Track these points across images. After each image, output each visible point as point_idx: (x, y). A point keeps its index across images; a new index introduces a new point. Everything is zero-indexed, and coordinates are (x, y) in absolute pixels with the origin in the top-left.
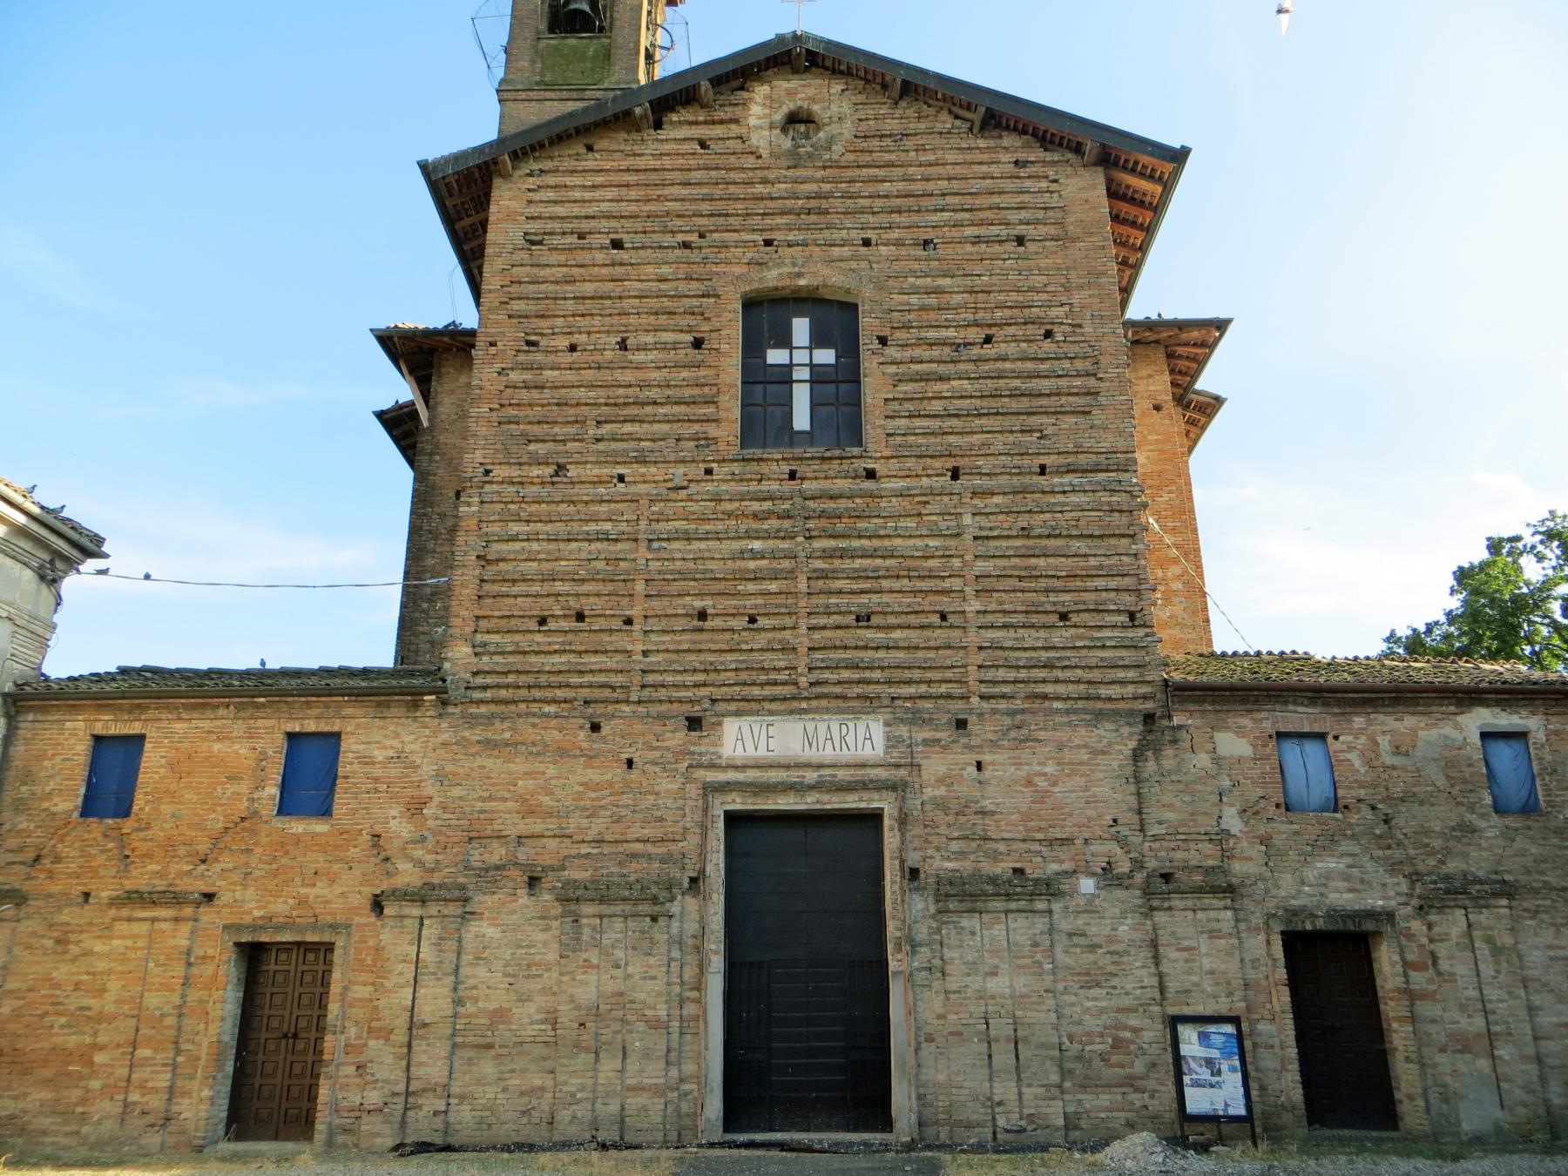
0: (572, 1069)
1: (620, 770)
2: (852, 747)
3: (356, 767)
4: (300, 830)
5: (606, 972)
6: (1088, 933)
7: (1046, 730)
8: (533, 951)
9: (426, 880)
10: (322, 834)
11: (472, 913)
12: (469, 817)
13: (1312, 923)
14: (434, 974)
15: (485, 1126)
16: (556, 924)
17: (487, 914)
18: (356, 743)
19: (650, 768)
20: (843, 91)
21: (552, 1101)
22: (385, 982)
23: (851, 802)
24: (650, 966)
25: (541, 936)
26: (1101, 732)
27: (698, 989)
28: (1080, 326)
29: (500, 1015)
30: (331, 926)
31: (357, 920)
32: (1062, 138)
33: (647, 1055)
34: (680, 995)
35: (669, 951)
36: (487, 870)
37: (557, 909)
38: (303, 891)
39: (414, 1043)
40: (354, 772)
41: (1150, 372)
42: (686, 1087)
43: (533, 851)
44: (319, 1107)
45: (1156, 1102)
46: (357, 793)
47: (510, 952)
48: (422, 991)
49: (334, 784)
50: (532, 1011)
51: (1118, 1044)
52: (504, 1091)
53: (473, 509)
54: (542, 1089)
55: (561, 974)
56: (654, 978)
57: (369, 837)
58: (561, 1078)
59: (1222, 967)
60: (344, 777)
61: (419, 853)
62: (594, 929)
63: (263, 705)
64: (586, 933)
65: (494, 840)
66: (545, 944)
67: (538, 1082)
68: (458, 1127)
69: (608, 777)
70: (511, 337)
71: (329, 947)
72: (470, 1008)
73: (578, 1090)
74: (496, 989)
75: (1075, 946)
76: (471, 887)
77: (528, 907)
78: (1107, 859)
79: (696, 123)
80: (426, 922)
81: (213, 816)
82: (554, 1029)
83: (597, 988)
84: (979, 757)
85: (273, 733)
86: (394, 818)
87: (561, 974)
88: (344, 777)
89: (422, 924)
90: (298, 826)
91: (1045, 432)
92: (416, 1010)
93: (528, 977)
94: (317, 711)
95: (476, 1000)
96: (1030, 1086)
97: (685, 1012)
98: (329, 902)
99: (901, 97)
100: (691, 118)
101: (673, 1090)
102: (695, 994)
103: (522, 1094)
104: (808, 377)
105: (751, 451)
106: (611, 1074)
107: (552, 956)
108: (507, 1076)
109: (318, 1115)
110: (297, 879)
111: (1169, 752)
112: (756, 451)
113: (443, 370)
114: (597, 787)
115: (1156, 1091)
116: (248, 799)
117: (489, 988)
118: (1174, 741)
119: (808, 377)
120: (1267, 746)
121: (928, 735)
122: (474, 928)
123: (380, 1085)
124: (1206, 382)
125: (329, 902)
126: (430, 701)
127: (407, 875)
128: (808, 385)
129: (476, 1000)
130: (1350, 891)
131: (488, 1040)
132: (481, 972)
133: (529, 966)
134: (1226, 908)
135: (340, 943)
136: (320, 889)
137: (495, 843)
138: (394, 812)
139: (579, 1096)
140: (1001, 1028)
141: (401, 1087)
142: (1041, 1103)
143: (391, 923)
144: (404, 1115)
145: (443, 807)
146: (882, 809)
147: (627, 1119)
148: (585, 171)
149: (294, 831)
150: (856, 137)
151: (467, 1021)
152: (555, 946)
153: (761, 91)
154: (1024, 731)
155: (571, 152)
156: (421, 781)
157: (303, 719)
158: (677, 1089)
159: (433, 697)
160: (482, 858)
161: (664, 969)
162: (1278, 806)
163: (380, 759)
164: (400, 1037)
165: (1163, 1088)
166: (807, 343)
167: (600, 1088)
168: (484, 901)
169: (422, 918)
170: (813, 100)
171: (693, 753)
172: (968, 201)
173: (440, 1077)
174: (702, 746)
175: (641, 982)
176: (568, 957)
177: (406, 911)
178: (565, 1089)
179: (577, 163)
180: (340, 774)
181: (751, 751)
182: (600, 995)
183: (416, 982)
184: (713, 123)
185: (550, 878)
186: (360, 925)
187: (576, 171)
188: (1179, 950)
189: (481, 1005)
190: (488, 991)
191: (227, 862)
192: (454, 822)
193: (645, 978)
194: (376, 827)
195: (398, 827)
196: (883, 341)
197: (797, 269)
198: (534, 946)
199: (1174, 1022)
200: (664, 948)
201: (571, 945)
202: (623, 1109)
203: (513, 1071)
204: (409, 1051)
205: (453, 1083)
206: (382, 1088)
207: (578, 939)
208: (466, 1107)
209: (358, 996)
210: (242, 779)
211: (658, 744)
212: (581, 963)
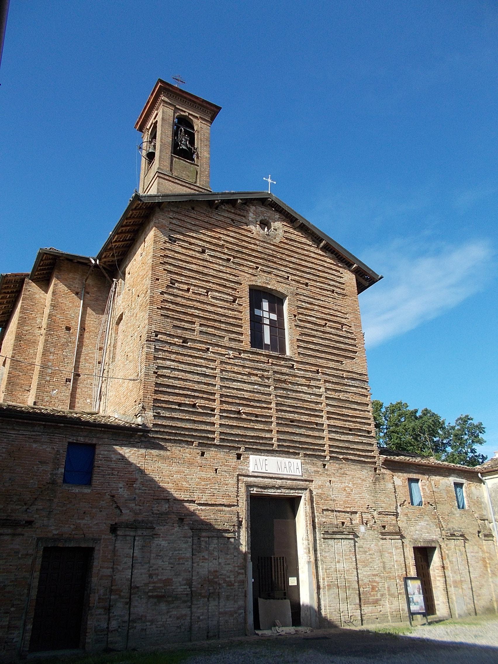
0: (198, 606)
1: (213, 474)
2: (293, 472)
3: (103, 462)
4: (77, 491)
5: (211, 562)
6: (364, 547)
7: (349, 471)
8: (181, 552)
13: (420, 544)
14: (140, 563)
15: (162, 635)
17: (162, 535)
18: (103, 450)
22: (118, 567)
24: (227, 559)
25: (184, 546)
26: (363, 473)
28: (351, 327)
29: (168, 582)
31: (103, 536)
37: (190, 533)
39: (132, 596)
40: (102, 464)
44: (88, 631)
45: (383, 609)
46: (104, 475)
47: (171, 553)
48: (135, 571)
50: (181, 580)
51: (373, 588)
52: (170, 617)
53: (152, 350)
54: (185, 615)
56: (229, 564)
57: (109, 497)
58: (194, 610)
59: (399, 559)
60: (98, 467)
62: (206, 542)
66: (186, 549)
67: (184, 612)
69: (209, 476)
72: (155, 579)
74: (166, 570)
76: (155, 522)
77: (178, 532)
78: (366, 520)
79: (230, 212)
80: (137, 538)
81: (31, 481)
83: (208, 569)
86: (121, 488)
88: (98, 467)
89: (134, 540)
90: (76, 490)
91: (343, 362)
92: (133, 580)
93: (179, 564)
94: (85, 434)
95: (157, 575)
96: (351, 605)
100: (229, 210)
101: (236, 613)
103: (178, 618)
106: (213, 607)
111: (382, 482)
112: (258, 350)
114: (204, 479)
115: (383, 605)
116: (51, 474)
117: (162, 569)
121: (316, 469)
122: (156, 541)
123: (116, 617)
125: (91, 527)
127: (127, 516)
129: (157, 575)
130: (428, 533)
131: (163, 594)
132: (160, 562)
135: (97, 548)
137: (163, 502)
138: (121, 485)
142: (354, 611)
144: (128, 631)
145: (142, 484)
149: (74, 491)
151: (154, 585)
154: (343, 470)
155: (186, 208)
157: (78, 436)
160: (158, 508)
163: (114, 459)
164: (125, 593)
168: (161, 529)
169: (135, 537)
170: (269, 217)
171: (239, 469)
173: (143, 612)
174: (242, 467)
175: (224, 566)
182: (209, 572)
184: (236, 214)
185: (187, 520)
188: (388, 553)
189: (159, 577)
190: (162, 571)
191: (39, 505)
192: (147, 491)
193: (226, 564)
194: (112, 492)
195: (123, 492)
197: (267, 281)
198: (181, 550)
203: (173, 608)
204: (130, 600)
206: (118, 619)
207: (200, 547)
208: (154, 626)
210: (48, 463)
211: (227, 463)
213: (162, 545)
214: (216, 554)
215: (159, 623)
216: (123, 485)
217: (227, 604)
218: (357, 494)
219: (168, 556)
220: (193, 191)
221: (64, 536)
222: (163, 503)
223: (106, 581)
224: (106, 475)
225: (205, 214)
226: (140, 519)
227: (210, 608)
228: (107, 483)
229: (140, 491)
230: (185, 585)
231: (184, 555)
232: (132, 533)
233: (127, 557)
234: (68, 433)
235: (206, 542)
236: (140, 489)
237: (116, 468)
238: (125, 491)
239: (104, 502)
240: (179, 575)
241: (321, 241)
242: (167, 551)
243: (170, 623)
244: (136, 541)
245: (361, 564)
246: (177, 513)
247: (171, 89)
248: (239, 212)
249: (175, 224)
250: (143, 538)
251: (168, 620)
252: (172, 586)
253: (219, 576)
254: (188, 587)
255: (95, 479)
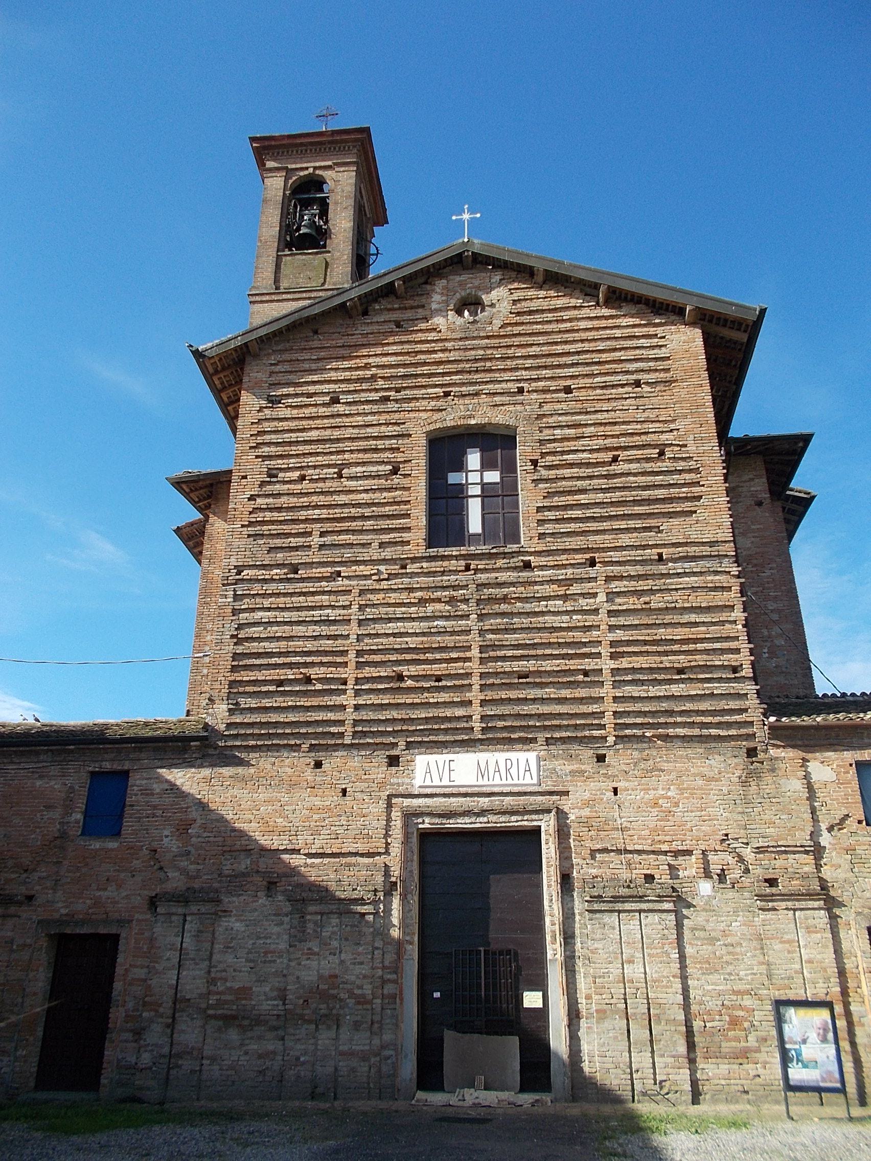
0: (297, 1037)
1: (337, 798)
2: (515, 777)
3: (140, 798)
5: (325, 958)
7: (668, 762)
8: (268, 941)
9: (188, 885)
10: (112, 850)
11: (225, 911)
12: (223, 835)
14: (193, 959)
16: (286, 919)
17: (235, 912)
19: (359, 796)
20: (501, 280)
21: (282, 1063)
22: (157, 965)
23: (515, 822)
25: (276, 929)
26: (712, 762)
27: (396, 973)
28: (686, 446)
29: (244, 993)
30: (118, 921)
31: (137, 916)
32: (668, 305)
33: (357, 1026)
34: (382, 977)
35: (373, 941)
36: (236, 876)
37: (287, 907)
38: (98, 894)
39: (177, 1015)
41: (751, 476)
42: (387, 1053)
43: (271, 861)
44: (105, 1065)
45: (768, 1071)
46: (140, 818)
47: (251, 942)
48: (184, 973)
49: (123, 811)
50: (267, 989)
51: (734, 1022)
52: (246, 1053)
53: (229, 600)
54: (274, 1053)
55: (290, 960)
56: (362, 963)
58: (289, 1044)
60: (131, 806)
61: (184, 864)
62: (315, 923)
63: (72, 751)
64: (310, 927)
65: (243, 853)
66: (279, 934)
68: (208, 1083)
69: (328, 803)
70: (256, 470)
71: (115, 938)
72: (220, 987)
73: (301, 1054)
74: (240, 971)
75: (697, 939)
77: (265, 906)
78: (721, 867)
80: (188, 918)
81: (33, 836)
82: (284, 1004)
83: (318, 971)
84: (615, 785)
85: (79, 772)
86: (167, 836)
87: (290, 960)
89: (185, 921)
90: (96, 845)
91: (661, 528)
92: (179, 988)
93: (265, 962)
95: (226, 980)
96: (662, 1056)
97: (386, 992)
98: (117, 903)
99: (544, 283)
100: (389, 306)
101: (376, 1055)
102: (394, 976)
104: (479, 493)
105: (435, 550)
106: (327, 1042)
107: (283, 946)
108: (247, 1042)
109: (103, 1072)
110: (93, 885)
111: (768, 778)
112: (441, 550)
113: (219, 496)
115: (766, 1063)
116: (60, 823)
117: (235, 970)
118: (773, 770)
119: (479, 493)
120: (848, 772)
121: (575, 767)
122: (224, 923)
124: (800, 483)
125: (117, 903)
126: (195, 746)
127: (175, 881)
128: (480, 499)
131: (233, 1013)
132: (230, 958)
133: (266, 953)
134: (820, 909)
135: (123, 935)
136: (110, 892)
138: (166, 833)
139: (302, 1059)
140: (638, 1007)
141: (166, 1050)
142: (671, 1071)
143: (162, 918)
144: (168, 1072)
145: (204, 827)
146: (540, 827)
147: (340, 1079)
148: (312, 349)
149: (92, 847)
150: (511, 313)
151: (218, 997)
152: (286, 937)
153: (441, 284)
154: (651, 762)
155: (301, 336)
156: (187, 808)
157: (102, 761)
158: (379, 1054)
159: (197, 743)
161: (370, 957)
162: (860, 822)
163: (158, 791)
164: (166, 1008)
165: (773, 1060)
166: (479, 468)
167: (319, 1053)
168: (232, 902)
169: (185, 915)
171: (392, 784)
172: (596, 357)
173: (196, 1042)
174: (397, 780)
175: (352, 967)
176: (295, 946)
177: (174, 910)
178: (292, 1053)
179: (306, 344)
180: (127, 803)
181: (436, 782)
182: (321, 977)
183: (179, 966)
184: (406, 309)
185: (283, 883)
186: (138, 920)
187: (305, 349)
188: (781, 942)
189: (228, 984)
190: (234, 974)
191: (43, 872)
192: (211, 839)
193: (354, 964)
194: (153, 844)
195: (170, 843)
196: (535, 463)
197: (468, 413)
199: (780, 1004)
200: (370, 938)
201: (298, 936)
202: (336, 1069)
203: (252, 1038)
204: (173, 1021)
205: (205, 1047)
206: (152, 1050)
209: (136, 976)
210: (56, 807)
212: (306, 951)
213: (235, 929)
214: (335, 944)
215: (226, 1062)
216: (171, 832)
218: (692, 812)
222: (242, 857)
225: (339, 333)
227: (320, 1042)
228: (144, 830)
229: (199, 839)
230: (275, 1000)
232: (180, 910)
233: (171, 949)
234: (86, 759)
235: (315, 923)
236: (199, 837)
237: (158, 805)
239: (138, 862)
240: (264, 981)
241: (596, 286)
242: (243, 938)
243: (245, 1063)
244: (187, 922)
245: (698, 966)
247: (273, 143)
249: (281, 372)
252: (251, 999)
254: (281, 1003)
255: (127, 826)
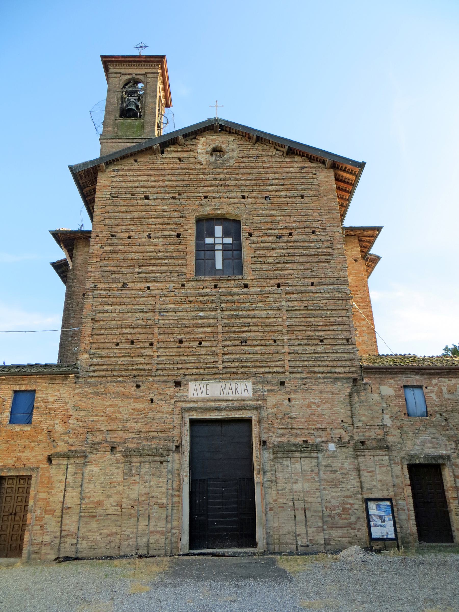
0: (128, 525)
1: (148, 403)
2: (240, 393)
3: (42, 404)
4: (19, 430)
6: (333, 466)
7: (315, 385)
8: (112, 477)
9: (69, 449)
10: (28, 431)
11: (88, 462)
12: (88, 423)
13: (419, 460)
14: (72, 487)
15: (92, 550)
16: (122, 466)
17: (94, 462)
18: (42, 394)
19: (160, 402)
20: (234, 140)
21: (120, 538)
22: (52, 491)
23: (240, 415)
24: (160, 482)
25: (116, 471)
26: (336, 386)
27: (179, 491)
28: (326, 229)
29: (99, 504)
30: (30, 468)
31: (41, 466)
32: (317, 158)
33: (158, 519)
34: (172, 494)
35: (167, 476)
36: (94, 444)
37: (122, 460)
38: (19, 454)
39: (64, 516)
40: (41, 406)
41: (352, 247)
42: (174, 531)
43: (113, 436)
44: (24, 543)
46: (42, 414)
47: (103, 477)
48: (68, 494)
49: (32, 411)
50: (112, 501)
52: (100, 534)
53: (90, 300)
54: (116, 533)
55: (124, 486)
56: (162, 487)
57: (46, 432)
58: (124, 529)
59: (385, 478)
60: (37, 408)
61: (67, 438)
62: (137, 467)
63: (4, 380)
64: (134, 469)
65: (98, 432)
66: (118, 474)
67: (114, 531)
68: (81, 550)
69: (143, 406)
70: (105, 233)
71: (30, 477)
72: (87, 501)
73: (130, 534)
74: (97, 493)
75: (328, 471)
76: (88, 451)
77: (111, 459)
78: (339, 436)
79: (177, 152)
80: (69, 466)
82: (121, 509)
83: (138, 491)
84: (289, 396)
85: (8, 391)
86: (57, 424)
87: (124, 486)
88: (37, 408)
89: (67, 467)
90: (18, 428)
91: (313, 270)
92: (65, 502)
93: (110, 488)
94: (26, 382)
95: (89, 497)
96: (310, 528)
97: (174, 501)
98: (30, 459)
99: (256, 142)
100: (175, 150)
102: (177, 493)
103: (108, 536)
104: (221, 248)
105: (199, 277)
106: (144, 527)
107: (120, 479)
108: (102, 528)
109: (24, 546)
110: (17, 450)
111: (363, 393)
113: (78, 246)
114: (139, 410)
115: (360, 529)
117: (94, 492)
118: (365, 389)
119: (221, 248)
120: (400, 391)
121: (269, 387)
122: (89, 468)
123: (49, 534)
124: (374, 251)
125: (30, 459)
126: (72, 377)
127: (62, 447)
128: (221, 251)
129: (89, 497)
130: (433, 447)
131: (94, 514)
132: (91, 486)
133: (111, 483)
134: (386, 455)
135: (34, 475)
136: (27, 454)
137: (98, 434)
139: (131, 536)
140: (299, 505)
141: (58, 534)
143: (55, 467)
144: (60, 545)
146: (252, 417)
147: (150, 545)
148: (134, 170)
149: (16, 430)
150: (239, 157)
151: (86, 506)
152: (122, 475)
153: (202, 140)
154: (307, 386)
155: (128, 162)
156: (68, 409)
157: (20, 385)
158: (171, 532)
159: (73, 375)
160: (92, 439)
161: (165, 483)
162: (405, 414)
163: (51, 400)
164: (58, 513)
165: (362, 528)
166: (221, 236)
167: (139, 533)
168: (92, 457)
169: (67, 465)
170: (222, 143)
171: (177, 396)
172: (282, 182)
173: (74, 530)
174: (181, 393)
176: (127, 479)
177: (61, 462)
178: (125, 533)
179: (131, 167)
180: (35, 407)
181: (200, 395)
182: (140, 495)
183: (65, 491)
184: (184, 151)
186: (42, 468)
187: (130, 170)
189: (91, 499)
192: (81, 425)
193: (158, 487)
194: (49, 428)
195: (59, 428)
196: (250, 234)
197: (217, 207)
198: (113, 475)
199: (367, 500)
200: (165, 475)
201: (128, 474)
202: (148, 541)
203: (104, 526)
205: (79, 532)
206: (50, 535)
207: (131, 472)
208: (85, 542)
209: (41, 497)
211: (163, 392)
212: (132, 481)
213: (94, 471)
214: (147, 477)
215: (90, 539)
216: (59, 422)
217: (158, 524)
218: (326, 409)
219: (99, 480)
220: (134, 144)
221: (7, 467)
222: (98, 434)
223: (43, 503)
224: (44, 414)
225: (149, 162)
226: (73, 449)
227: (140, 527)
228: (45, 421)
229: (75, 425)
230: (116, 506)
231: (115, 479)
232: (65, 462)
233: (60, 482)
234: (12, 383)
235: (137, 467)
236: (74, 424)
237: (53, 408)
238: (61, 427)
239: (41, 437)
240: (110, 497)
242: (99, 476)
243: (100, 539)
244: (69, 468)
245: (328, 484)
246: (110, 442)
247: (114, 59)
248: (187, 148)
249: (117, 181)
250: (76, 466)
251: (98, 537)
252: (103, 507)
253: (151, 498)
254: (119, 508)
255: (35, 419)
